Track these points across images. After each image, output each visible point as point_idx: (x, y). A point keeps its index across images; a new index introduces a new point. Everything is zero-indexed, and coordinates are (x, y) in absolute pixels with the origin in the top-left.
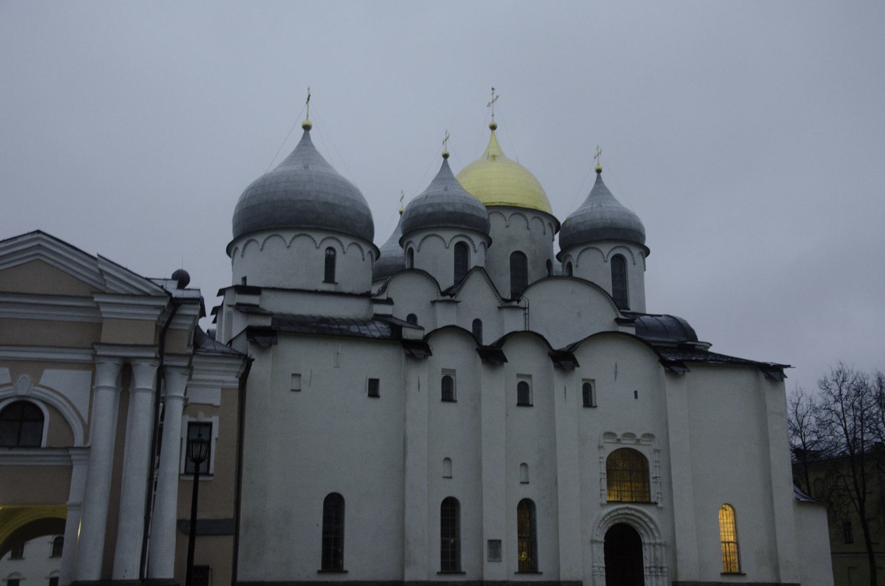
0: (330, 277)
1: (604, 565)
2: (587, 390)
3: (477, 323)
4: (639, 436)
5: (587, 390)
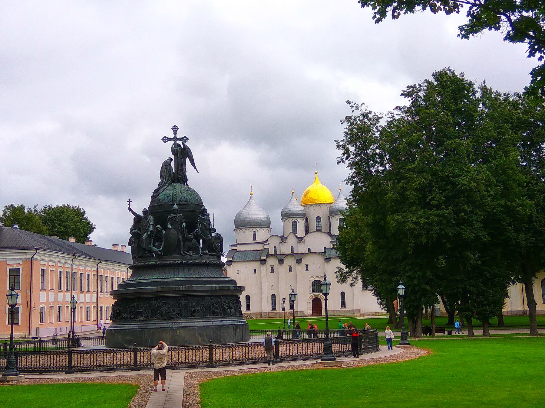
0: (255, 239)
1: (312, 307)
2: (307, 267)
3: (292, 247)
4: (320, 277)
5: (307, 267)
